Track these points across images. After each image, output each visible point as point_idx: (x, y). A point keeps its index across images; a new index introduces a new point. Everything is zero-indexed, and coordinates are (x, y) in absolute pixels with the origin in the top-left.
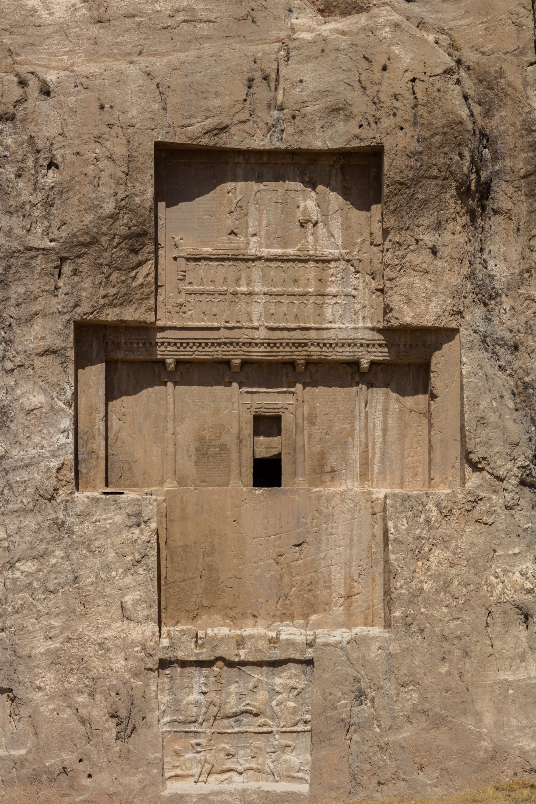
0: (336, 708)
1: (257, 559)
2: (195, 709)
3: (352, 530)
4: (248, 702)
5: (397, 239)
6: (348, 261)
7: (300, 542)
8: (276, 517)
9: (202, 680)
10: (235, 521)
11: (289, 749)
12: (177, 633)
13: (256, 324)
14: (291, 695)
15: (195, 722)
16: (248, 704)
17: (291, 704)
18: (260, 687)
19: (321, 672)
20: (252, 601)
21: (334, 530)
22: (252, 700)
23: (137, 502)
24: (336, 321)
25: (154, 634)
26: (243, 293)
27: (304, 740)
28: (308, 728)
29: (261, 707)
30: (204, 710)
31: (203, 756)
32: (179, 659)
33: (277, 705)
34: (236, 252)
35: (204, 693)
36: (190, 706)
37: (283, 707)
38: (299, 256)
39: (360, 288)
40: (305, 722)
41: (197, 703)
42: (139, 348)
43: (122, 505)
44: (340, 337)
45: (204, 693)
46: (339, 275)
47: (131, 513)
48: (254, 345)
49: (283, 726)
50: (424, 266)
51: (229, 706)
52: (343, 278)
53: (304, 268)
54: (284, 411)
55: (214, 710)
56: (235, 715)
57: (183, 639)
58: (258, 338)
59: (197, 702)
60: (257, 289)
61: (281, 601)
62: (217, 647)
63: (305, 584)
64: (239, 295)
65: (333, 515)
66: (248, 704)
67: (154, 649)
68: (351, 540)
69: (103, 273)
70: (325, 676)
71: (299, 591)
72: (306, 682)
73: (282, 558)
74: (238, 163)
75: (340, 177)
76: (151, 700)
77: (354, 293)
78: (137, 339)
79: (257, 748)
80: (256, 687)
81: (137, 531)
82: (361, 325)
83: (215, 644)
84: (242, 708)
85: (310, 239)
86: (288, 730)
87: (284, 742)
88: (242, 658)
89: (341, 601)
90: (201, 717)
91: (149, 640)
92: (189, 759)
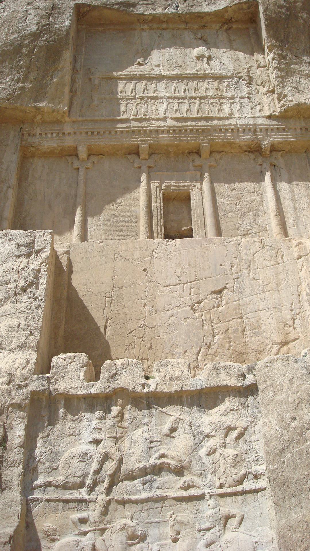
0: (306, 440)
1: (171, 307)
2: (82, 465)
3: (277, 275)
4: (161, 452)
5: (280, 52)
6: (240, 78)
7: (220, 288)
8: (189, 265)
9: (95, 423)
10: (145, 270)
11: (233, 523)
12: (61, 361)
13: (162, 115)
14: (228, 439)
15: (81, 485)
16: (163, 456)
17: (230, 452)
18: (180, 430)
19: (270, 395)
20: (167, 352)
21: (257, 275)
22: (169, 449)
23: (29, 234)
24: (235, 113)
25: (28, 362)
26: (148, 98)
27: (256, 504)
28: (263, 483)
29: (183, 458)
30: (94, 466)
31: (90, 539)
32: (61, 391)
33: (209, 455)
34: (141, 73)
35: (97, 442)
36: (76, 460)
37: (217, 454)
38: (197, 74)
39: (254, 92)
40: (256, 477)
41: (85, 457)
42: (53, 137)
43: (13, 237)
44: (240, 122)
45: (97, 442)
46: (233, 86)
47: (22, 243)
48: (161, 132)
49: (221, 486)
50: (307, 72)
51: (134, 458)
52: (236, 88)
53: (202, 83)
54: (193, 188)
55: (110, 466)
56: (144, 472)
57: (69, 368)
58: (164, 126)
59: (86, 454)
60: (162, 94)
61: (202, 350)
62: (117, 377)
63: (230, 331)
64: (145, 99)
65: (254, 261)
66: (163, 456)
67: (26, 379)
68: (278, 285)
69: (22, 72)
70: (278, 398)
71: (224, 339)
72: (250, 419)
73: (201, 305)
74: (143, 29)
75: (225, 35)
76: (12, 448)
77: (247, 95)
78: (50, 130)
79: (181, 523)
80: (173, 430)
81: (25, 261)
82: (258, 115)
83: (114, 372)
84: (153, 461)
85: (206, 66)
86: (229, 490)
87: (225, 510)
88: (152, 388)
89: (275, 348)
90: (90, 476)
91: (21, 367)
92: (67, 545)
